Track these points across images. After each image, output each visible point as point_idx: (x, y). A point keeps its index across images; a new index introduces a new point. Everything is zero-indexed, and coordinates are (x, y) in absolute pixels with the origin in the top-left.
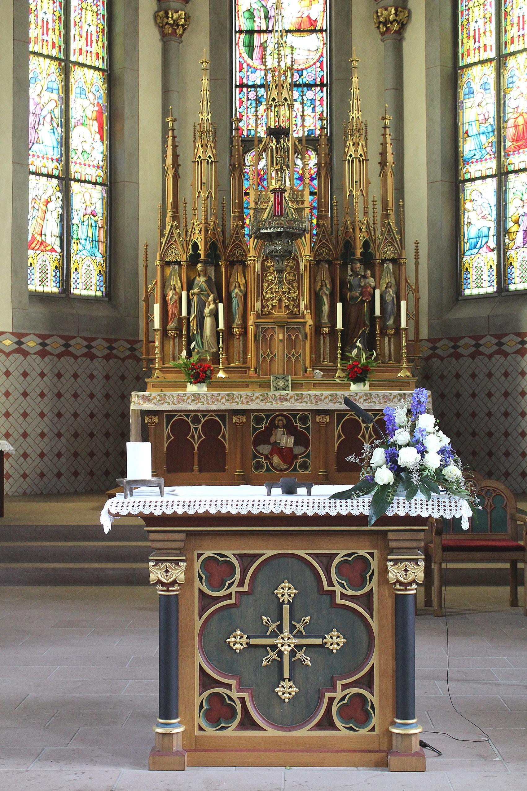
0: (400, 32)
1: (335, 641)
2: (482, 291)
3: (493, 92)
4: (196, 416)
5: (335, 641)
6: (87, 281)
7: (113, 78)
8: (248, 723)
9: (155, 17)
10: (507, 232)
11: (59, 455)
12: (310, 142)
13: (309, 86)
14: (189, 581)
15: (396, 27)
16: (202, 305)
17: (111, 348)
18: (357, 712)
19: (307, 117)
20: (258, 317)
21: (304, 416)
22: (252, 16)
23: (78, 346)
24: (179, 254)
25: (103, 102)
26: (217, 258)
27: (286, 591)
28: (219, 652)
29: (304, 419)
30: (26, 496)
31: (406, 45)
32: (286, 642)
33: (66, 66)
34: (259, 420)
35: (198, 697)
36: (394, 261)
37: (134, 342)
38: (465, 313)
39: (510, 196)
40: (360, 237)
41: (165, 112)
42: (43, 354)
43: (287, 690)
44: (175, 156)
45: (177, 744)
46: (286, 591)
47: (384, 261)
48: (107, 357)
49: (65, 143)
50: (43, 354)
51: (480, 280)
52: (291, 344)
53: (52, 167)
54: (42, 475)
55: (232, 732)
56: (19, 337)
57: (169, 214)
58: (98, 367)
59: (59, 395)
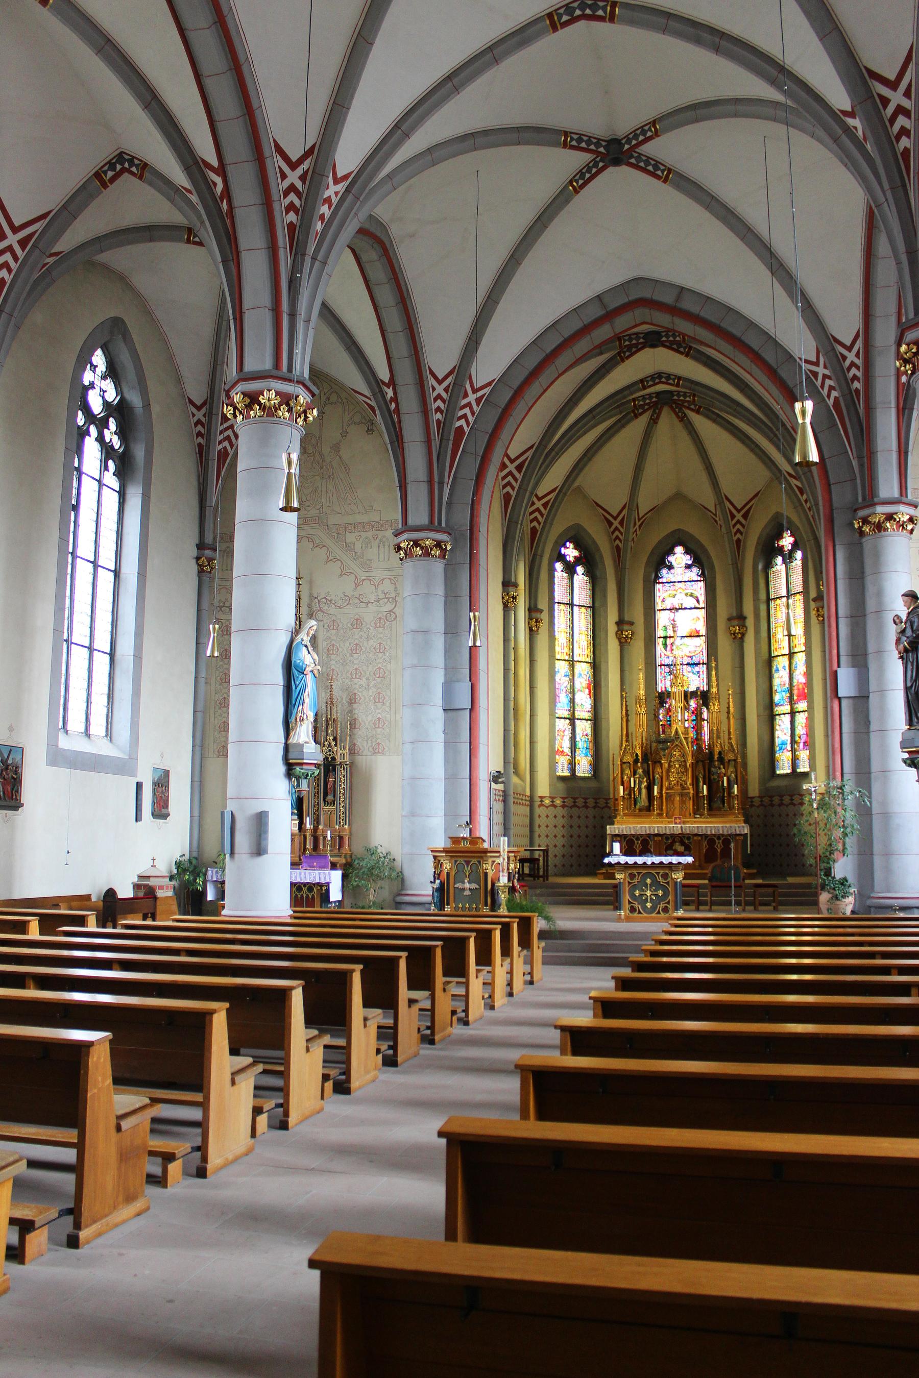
0: (742, 639)
1: (660, 893)
2: (785, 772)
3: (788, 670)
4: (637, 837)
5: (660, 893)
6: (584, 768)
7: (595, 666)
8: (640, 912)
9: (616, 634)
10: (796, 742)
11: (572, 856)
13: (696, 664)
14: (624, 880)
15: (740, 636)
16: (640, 783)
17: (596, 803)
18: (666, 910)
19: (695, 681)
20: (667, 789)
21: (689, 837)
22: (666, 628)
23: (580, 802)
24: (628, 758)
25: (591, 679)
26: (648, 760)
27: (649, 881)
28: (632, 895)
29: (689, 838)
30: (556, 875)
31: (745, 645)
32: (648, 893)
33: (572, 663)
34: (667, 839)
35: (627, 906)
36: (734, 760)
37: (607, 799)
38: (775, 783)
39: (796, 724)
40: (717, 750)
41: (622, 690)
42: (563, 806)
43: (649, 905)
44: (627, 711)
45: (623, 917)
46: (649, 881)
47: (729, 760)
48: (594, 807)
49: (572, 701)
50: (563, 806)
51: (784, 768)
52: (683, 802)
53: (566, 714)
54: (564, 865)
55: (636, 914)
56: (552, 798)
57: (624, 739)
58: (591, 812)
59: (571, 827)
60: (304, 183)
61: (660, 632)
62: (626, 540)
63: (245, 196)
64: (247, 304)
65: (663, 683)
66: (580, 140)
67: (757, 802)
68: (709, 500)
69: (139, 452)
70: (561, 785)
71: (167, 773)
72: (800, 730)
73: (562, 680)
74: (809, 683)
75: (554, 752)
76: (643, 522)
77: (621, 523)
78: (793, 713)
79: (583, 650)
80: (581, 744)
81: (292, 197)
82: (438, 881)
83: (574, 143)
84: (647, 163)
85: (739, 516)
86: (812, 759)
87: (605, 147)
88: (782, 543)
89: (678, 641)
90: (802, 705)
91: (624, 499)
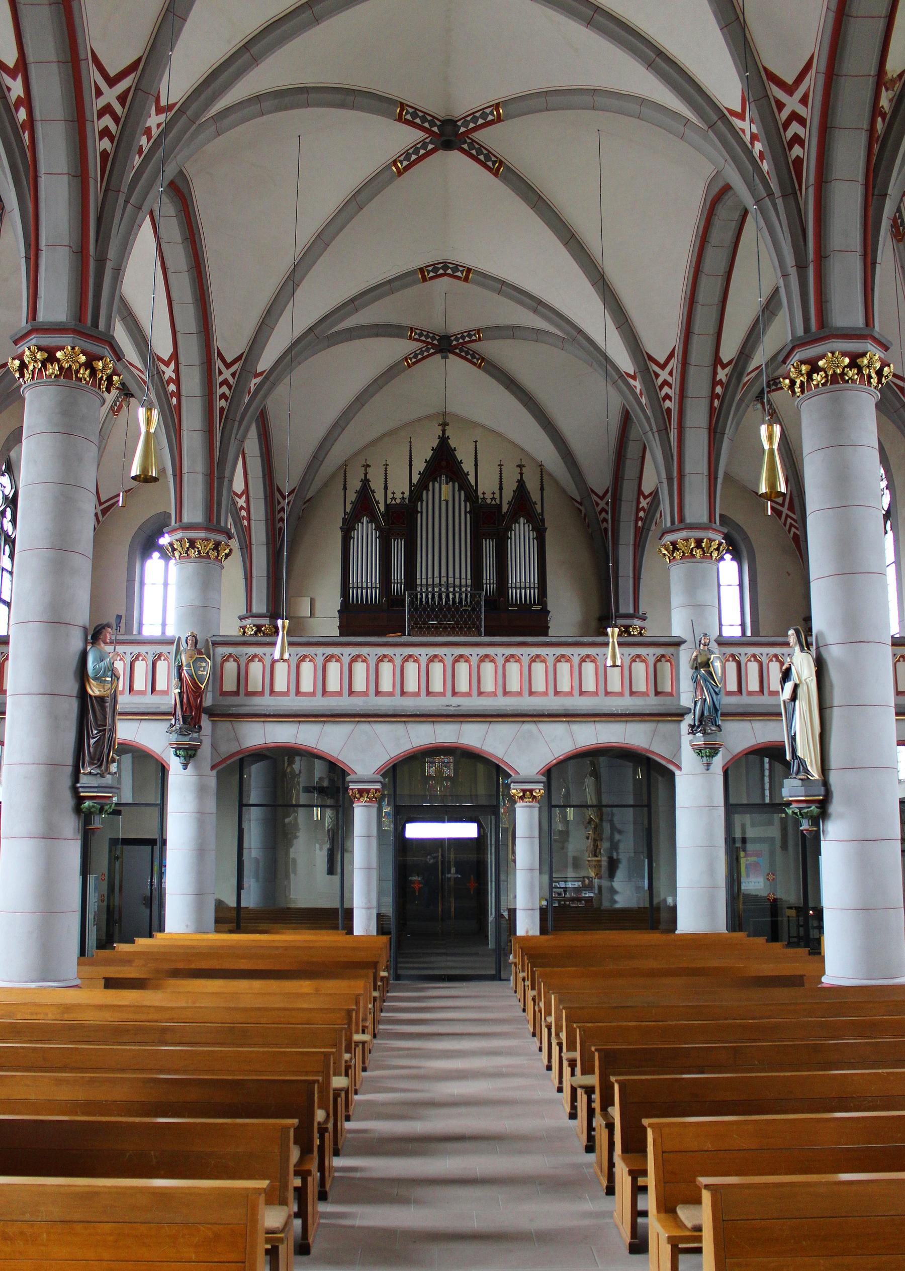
60: (234, 378)
63: (192, 383)
64: (185, 469)
66: (421, 335)
81: (225, 389)
83: (417, 337)
84: (467, 353)
87: (438, 341)
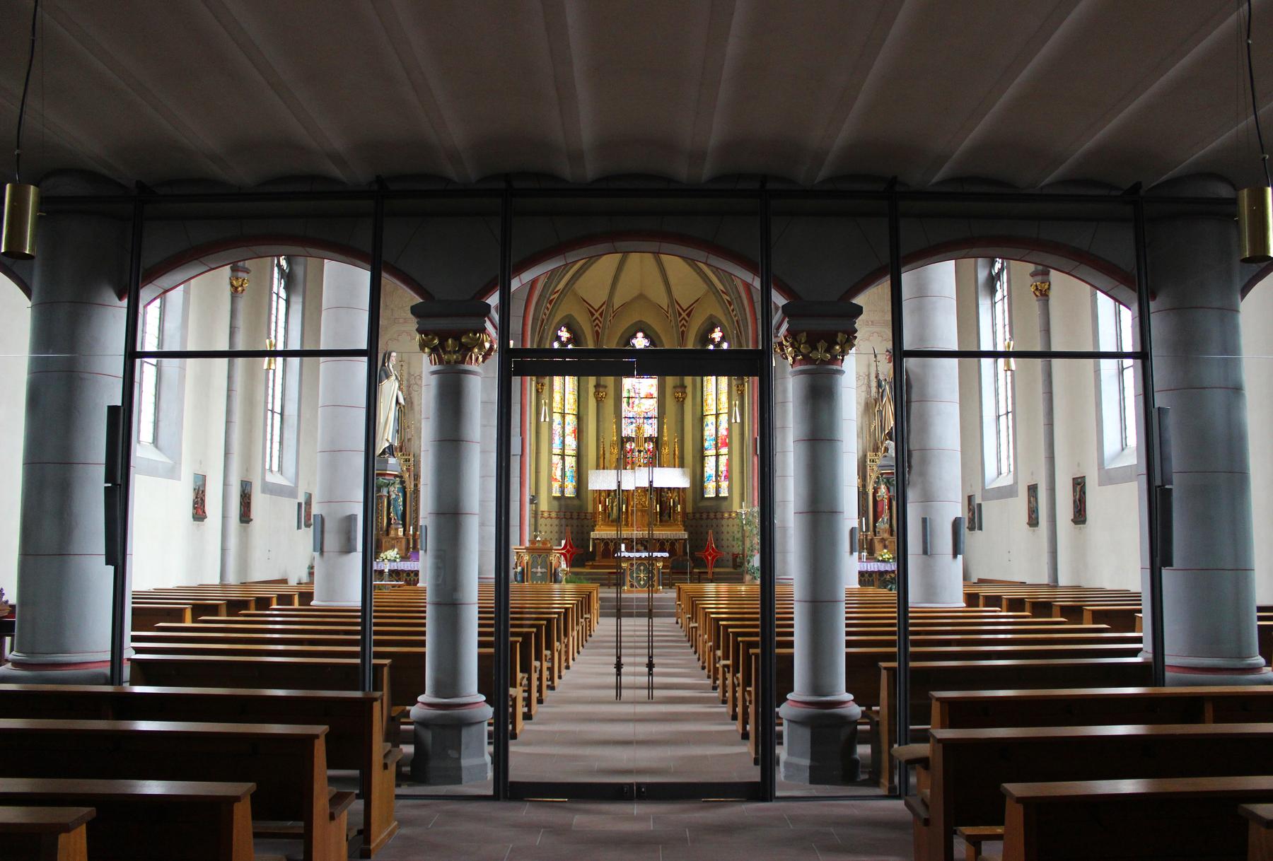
4: (612, 540)
6: (570, 491)
7: (579, 417)
12: (650, 439)
19: (650, 430)
23: (568, 515)
33: (563, 415)
49: (563, 442)
51: (710, 493)
58: (575, 522)
61: (625, 394)
62: (604, 328)
65: (628, 430)
67: (691, 516)
68: (664, 302)
69: (299, 271)
70: (556, 503)
71: (310, 495)
72: (722, 468)
73: (557, 427)
74: (729, 435)
75: (551, 478)
76: (616, 314)
77: (601, 314)
78: (717, 456)
79: (571, 406)
80: (568, 474)
82: (519, 569)
85: (684, 315)
86: (730, 488)
88: (714, 335)
89: (637, 401)
90: (724, 451)
91: (605, 298)
